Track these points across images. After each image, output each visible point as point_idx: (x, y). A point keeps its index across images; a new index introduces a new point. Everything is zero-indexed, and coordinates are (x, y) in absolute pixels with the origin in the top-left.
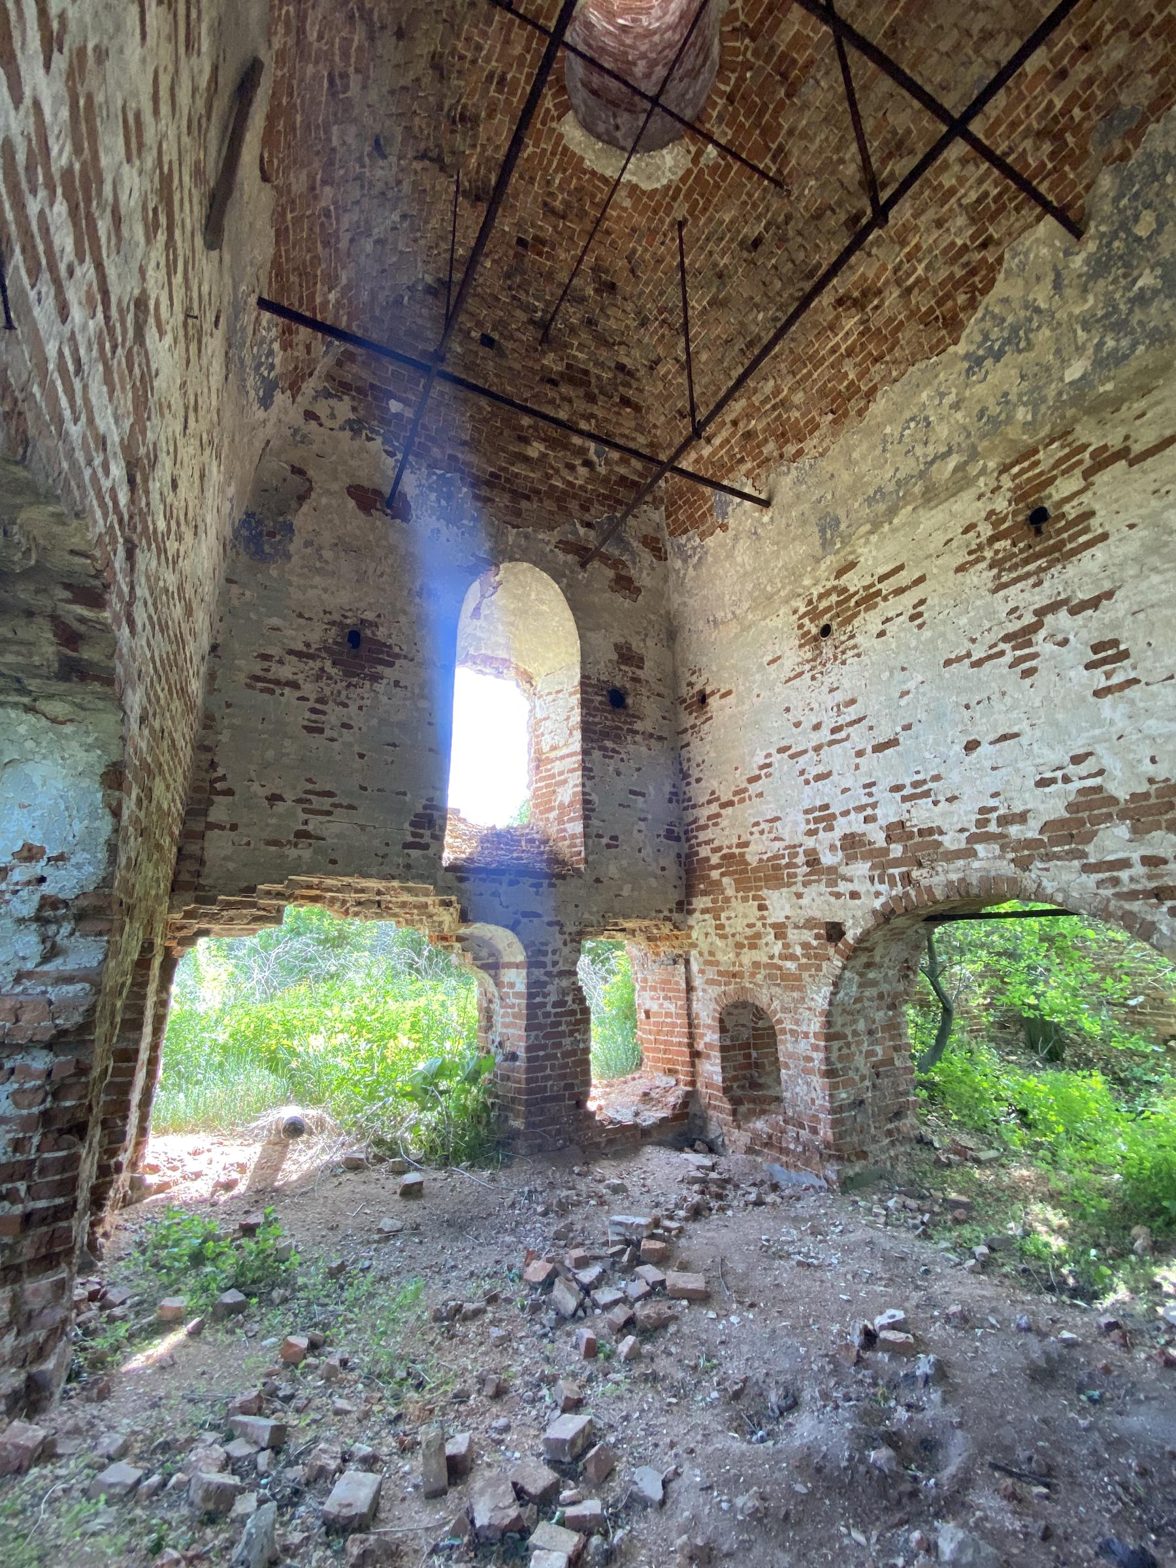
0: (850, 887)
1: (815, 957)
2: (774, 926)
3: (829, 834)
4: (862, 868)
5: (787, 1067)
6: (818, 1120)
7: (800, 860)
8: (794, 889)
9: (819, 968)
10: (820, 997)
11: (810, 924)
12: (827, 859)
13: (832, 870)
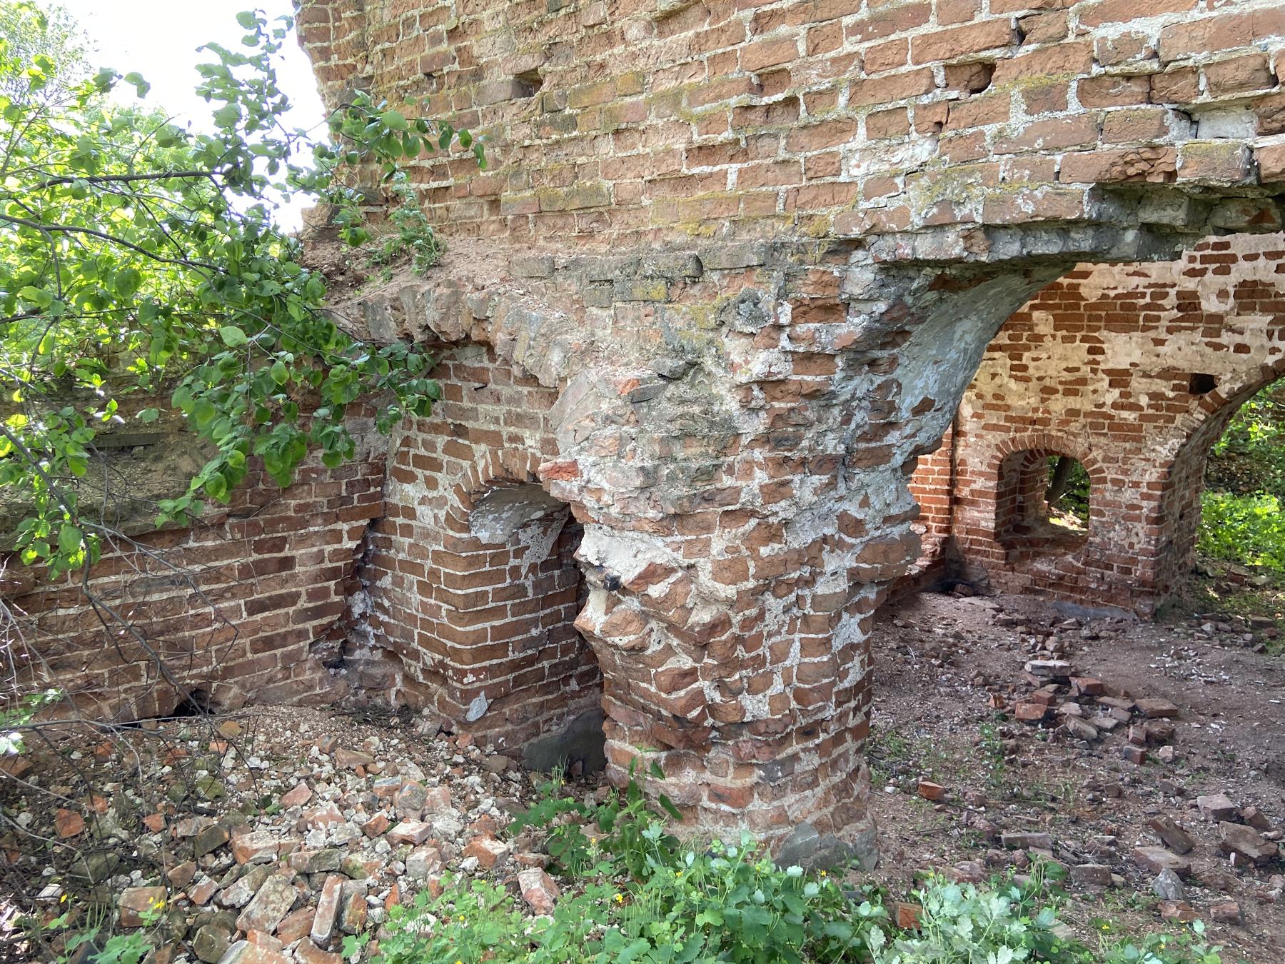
0: (1238, 339)
1: (1163, 409)
2: (1108, 372)
3: (1221, 279)
4: (1260, 321)
5: (1100, 513)
6: (1134, 561)
7: (1171, 301)
8: (1152, 334)
9: (1172, 420)
10: (1165, 448)
11: (1167, 374)
12: (1210, 305)
13: (1216, 318)
